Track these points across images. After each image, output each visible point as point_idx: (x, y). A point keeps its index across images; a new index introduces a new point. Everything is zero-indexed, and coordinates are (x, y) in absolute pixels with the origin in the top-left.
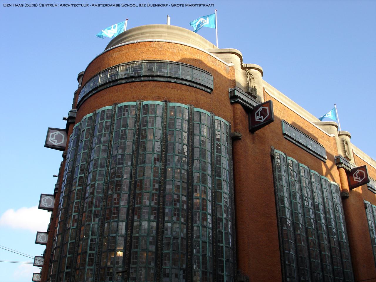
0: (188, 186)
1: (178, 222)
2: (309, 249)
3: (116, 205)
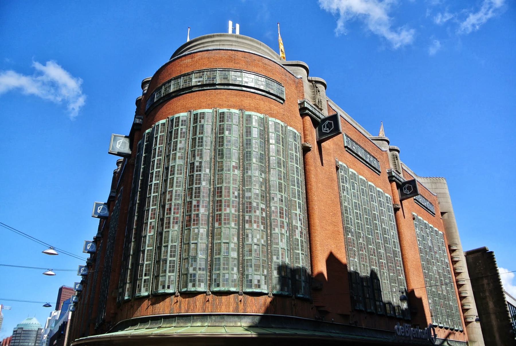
3: (196, 212)
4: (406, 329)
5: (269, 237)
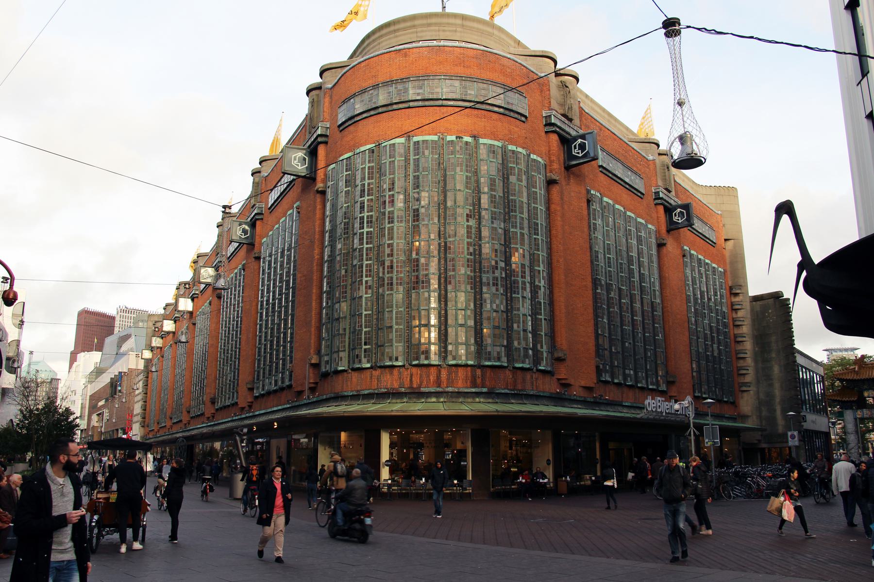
0: (505, 249)
2: (621, 314)
3: (425, 272)
4: (658, 404)
5: (509, 302)
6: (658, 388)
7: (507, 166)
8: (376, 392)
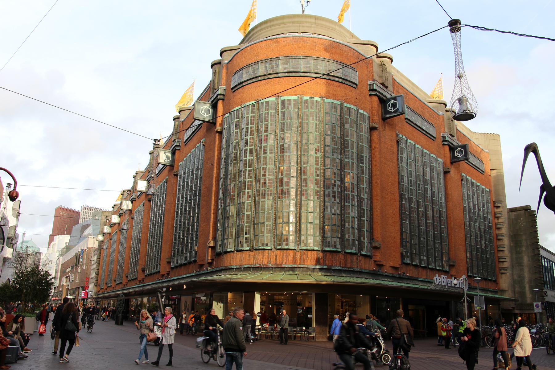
0: (341, 173)
1: (335, 202)
2: (418, 218)
3: (287, 187)
4: (443, 280)
5: (342, 208)
6: (443, 269)
7: (343, 117)
8: (252, 266)
